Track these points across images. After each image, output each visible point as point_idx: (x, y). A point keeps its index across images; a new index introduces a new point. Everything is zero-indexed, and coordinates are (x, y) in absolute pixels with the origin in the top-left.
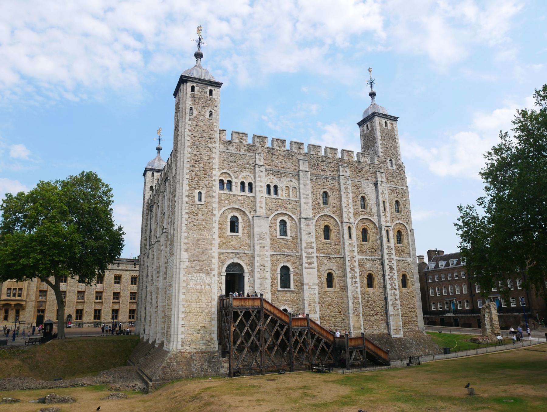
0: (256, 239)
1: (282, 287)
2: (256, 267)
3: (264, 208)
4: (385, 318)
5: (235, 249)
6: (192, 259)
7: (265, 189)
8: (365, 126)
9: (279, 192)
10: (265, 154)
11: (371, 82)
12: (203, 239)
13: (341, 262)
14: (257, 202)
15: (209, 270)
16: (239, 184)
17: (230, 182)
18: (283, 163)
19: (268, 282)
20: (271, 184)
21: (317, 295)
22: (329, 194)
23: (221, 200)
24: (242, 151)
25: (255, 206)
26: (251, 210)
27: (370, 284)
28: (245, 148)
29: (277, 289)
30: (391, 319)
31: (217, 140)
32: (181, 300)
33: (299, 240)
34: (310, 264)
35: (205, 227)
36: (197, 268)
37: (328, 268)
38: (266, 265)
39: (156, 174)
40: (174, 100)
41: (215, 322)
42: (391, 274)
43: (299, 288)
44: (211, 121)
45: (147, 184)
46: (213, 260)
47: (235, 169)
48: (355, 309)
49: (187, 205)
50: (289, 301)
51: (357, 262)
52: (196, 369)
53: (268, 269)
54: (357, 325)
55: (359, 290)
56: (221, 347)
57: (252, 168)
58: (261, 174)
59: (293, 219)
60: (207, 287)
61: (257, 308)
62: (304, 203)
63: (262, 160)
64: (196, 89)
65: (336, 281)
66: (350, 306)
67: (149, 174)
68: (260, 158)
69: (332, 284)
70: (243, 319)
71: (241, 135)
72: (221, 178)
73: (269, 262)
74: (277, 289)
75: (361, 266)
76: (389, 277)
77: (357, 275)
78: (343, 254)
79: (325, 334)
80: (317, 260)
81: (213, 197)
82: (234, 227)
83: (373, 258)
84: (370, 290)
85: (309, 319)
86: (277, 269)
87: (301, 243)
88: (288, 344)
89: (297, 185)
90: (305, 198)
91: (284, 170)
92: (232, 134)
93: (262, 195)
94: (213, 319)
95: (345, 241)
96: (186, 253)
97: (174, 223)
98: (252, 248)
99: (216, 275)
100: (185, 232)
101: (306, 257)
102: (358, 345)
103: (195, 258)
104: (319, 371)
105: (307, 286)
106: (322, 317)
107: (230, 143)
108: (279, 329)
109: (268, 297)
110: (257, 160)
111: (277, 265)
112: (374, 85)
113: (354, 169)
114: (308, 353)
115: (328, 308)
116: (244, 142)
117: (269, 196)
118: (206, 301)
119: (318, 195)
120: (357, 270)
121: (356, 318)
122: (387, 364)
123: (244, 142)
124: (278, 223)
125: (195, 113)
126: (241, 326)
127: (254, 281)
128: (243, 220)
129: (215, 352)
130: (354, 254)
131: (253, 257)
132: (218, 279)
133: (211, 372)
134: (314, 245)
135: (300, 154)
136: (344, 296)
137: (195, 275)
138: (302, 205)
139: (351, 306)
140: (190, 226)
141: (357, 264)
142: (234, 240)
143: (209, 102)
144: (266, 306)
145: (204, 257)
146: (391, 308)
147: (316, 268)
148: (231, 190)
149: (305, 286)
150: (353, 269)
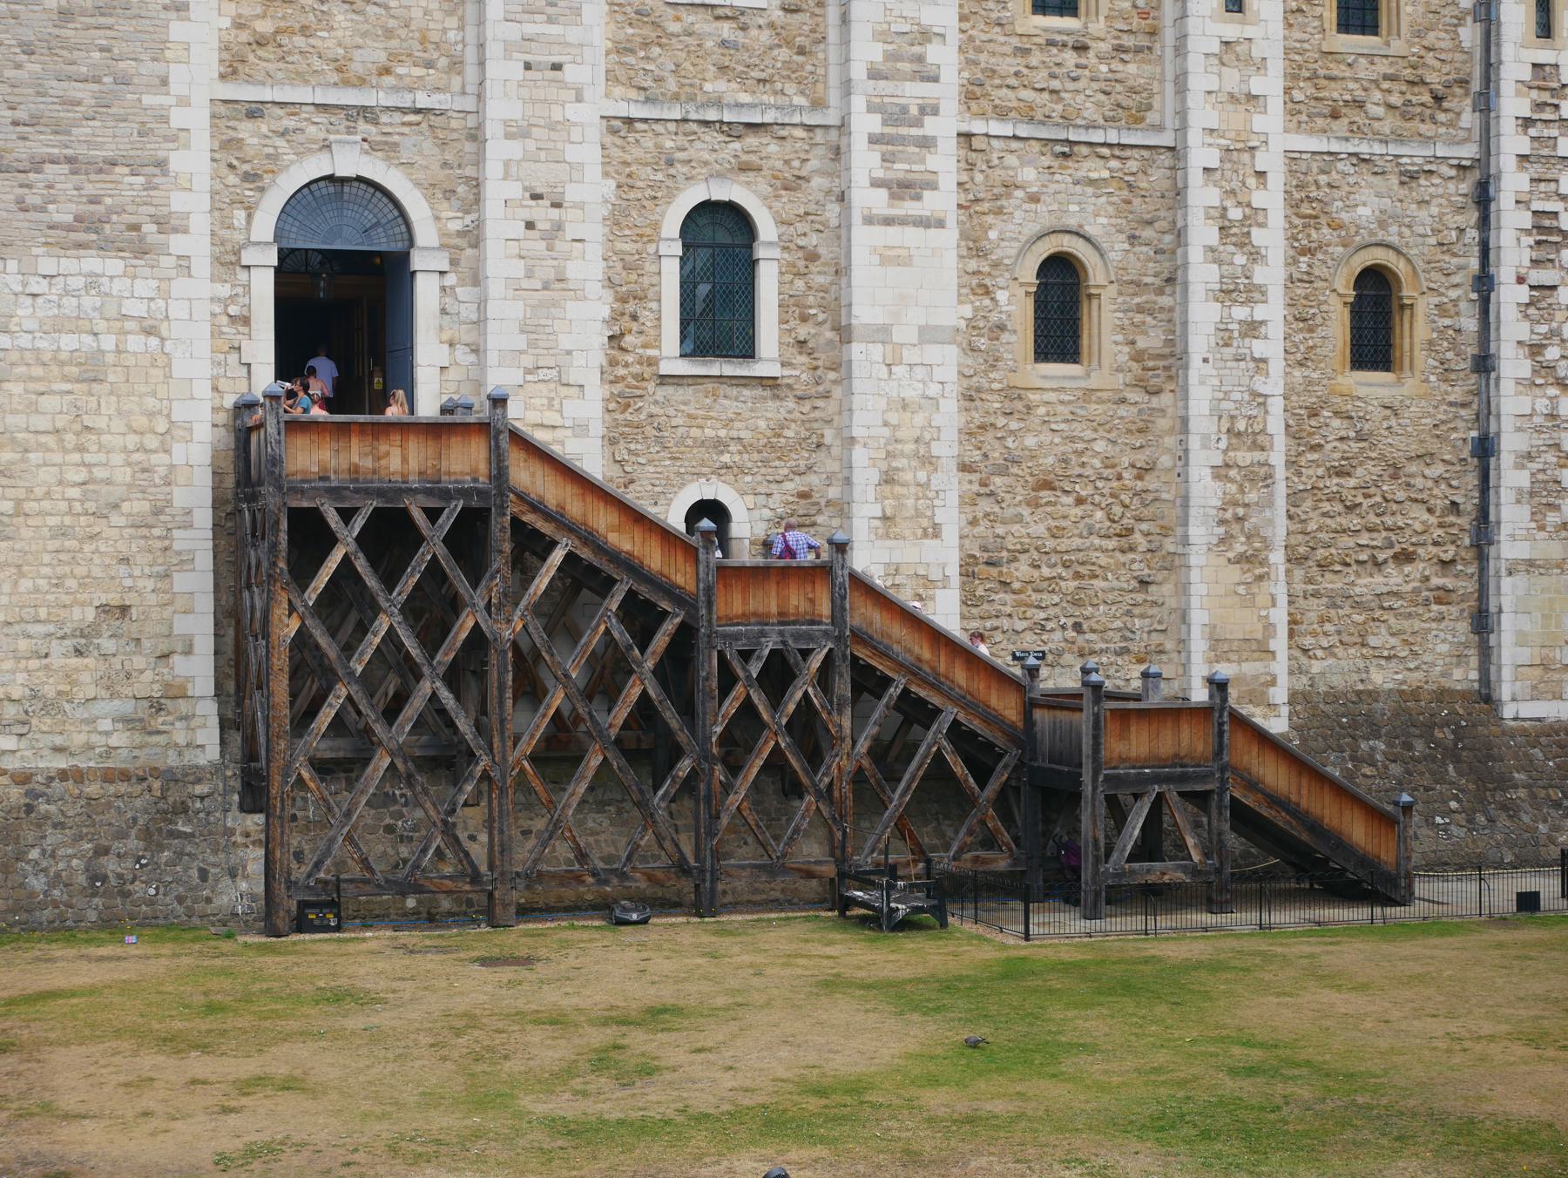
4: (1470, 586)
5: (346, 83)
13: (1157, 177)
15: (149, 228)
19: (585, 324)
27: (1373, 344)
29: (652, 362)
30: (1509, 592)
34: (904, 188)
37: (1047, 221)
38: (572, 194)
41: (197, 583)
42: (1537, 276)
43: (823, 359)
46: (178, 161)
48: (1233, 518)
50: (746, 448)
51: (1277, 180)
52: (56, 880)
54: (1242, 623)
55: (1273, 384)
56: (236, 738)
60: (135, 343)
61: (464, 493)
66: (1196, 491)
69: (1076, 336)
70: (361, 564)
73: (594, 171)
74: (652, 362)
75: (1307, 208)
76: (1523, 294)
77: (1272, 274)
78: (1171, 122)
79: (960, 676)
80: (971, 167)
83: (1414, 153)
84: (1372, 385)
85: (842, 576)
86: (656, 226)
87: (845, 42)
88: (683, 737)
94: (186, 562)
95: (1193, 24)
98: (471, 72)
99: (202, 265)
101: (874, 140)
102: (1177, 760)
103: (42, 144)
104: (879, 922)
105: (877, 351)
106: (982, 569)
108: (620, 634)
111: (659, 196)
114: (827, 795)
115: (1034, 504)
118: (132, 440)
120: (1272, 238)
121: (1235, 573)
122: (1372, 886)
126: (346, 603)
127: (482, 304)
129: (195, 775)
130: (1259, 123)
131: (476, 136)
132: (225, 290)
133: (151, 902)
134: (945, 57)
136: (1163, 423)
137: (47, 265)
139: (1205, 491)
141: (1272, 199)
144: (524, 475)
145: (105, 139)
146: (1511, 516)
147: (952, 218)
149: (857, 350)
150: (1236, 234)
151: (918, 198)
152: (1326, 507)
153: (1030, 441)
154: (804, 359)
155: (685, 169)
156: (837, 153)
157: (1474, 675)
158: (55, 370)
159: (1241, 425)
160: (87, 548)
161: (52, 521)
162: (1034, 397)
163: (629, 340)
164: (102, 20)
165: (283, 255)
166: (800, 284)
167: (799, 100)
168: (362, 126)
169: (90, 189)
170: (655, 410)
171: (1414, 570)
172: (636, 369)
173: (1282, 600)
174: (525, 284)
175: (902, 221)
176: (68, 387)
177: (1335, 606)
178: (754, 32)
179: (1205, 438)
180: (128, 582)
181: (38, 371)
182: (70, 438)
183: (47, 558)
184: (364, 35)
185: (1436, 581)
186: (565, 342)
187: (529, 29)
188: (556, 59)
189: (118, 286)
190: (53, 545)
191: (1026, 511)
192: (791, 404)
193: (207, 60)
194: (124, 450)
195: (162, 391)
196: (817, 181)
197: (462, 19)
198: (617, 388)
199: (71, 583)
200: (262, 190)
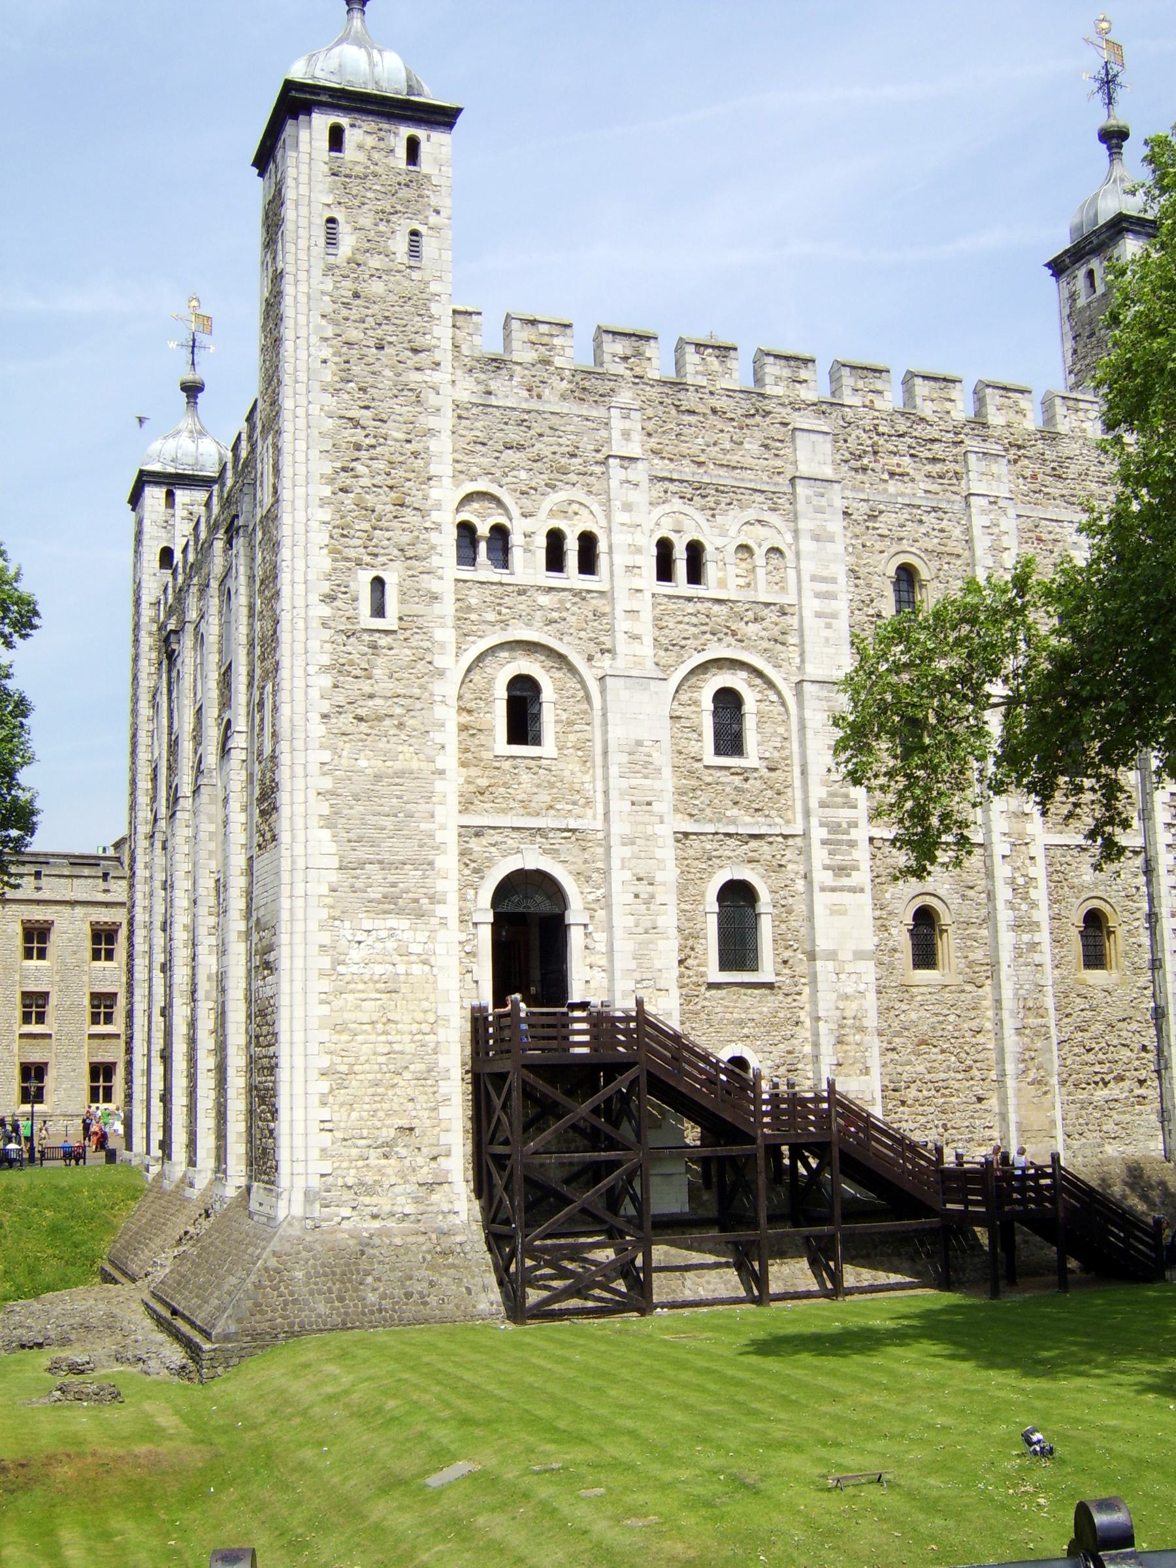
0: (614, 771)
1: (725, 965)
2: (616, 887)
3: (648, 640)
5: (529, 814)
6: (353, 856)
7: (649, 562)
8: (1081, 273)
9: (711, 571)
10: (650, 412)
11: (1108, 83)
12: (400, 774)
14: (619, 613)
16: (541, 541)
17: (500, 534)
18: (728, 445)
19: (668, 950)
20: (673, 537)
21: (871, 1001)
22: (925, 574)
23: (464, 610)
24: (551, 402)
25: (611, 631)
26: (593, 648)
28: (564, 385)
29: (703, 975)
31: (444, 354)
32: (314, 1023)
33: (797, 770)
34: (841, 870)
35: (401, 725)
36: (375, 893)
38: (659, 877)
39: (181, 496)
40: (255, 189)
44: (415, 275)
45: (146, 538)
46: (440, 862)
47: (523, 475)
48: (1027, 1058)
49: (327, 634)
51: (1041, 861)
53: (667, 896)
54: (1037, 1120)
57: (598, 469)
58: (634, 496)
59: (770, 684)
60: (417, 969)
62: (818, 615)
63: (637, 436)
64: (351, 137)
65: (948, 946)
67: (154, 495)
68: (627, 424)
71: (543, 328)
72: (464, 516)
73: (671, 864)
75: (1058, 877)
77: (1042, 915)
81: (435, 598)
82: (523, 719)
84: (1096, 976)
86: (703, 894)
89: (784, 541)
90: (818, 595)
91: (725, 478)
92: (506, 326)
93: (637, 583)
96: (326, 834)
97: (275, 709)
99: (454, 922)
100: (322, 747)
101: (824, 842)
103: (363, 853)
105: (830, 965)
106: (892, 1090)
107: (497, 364)
109: (667, 1009)
110: (616, 435)
111: (705, 875)
112: (1119, 95)
113: (1029, 467)
116: (558, 362)
117: (665, 588)
119: (876, 582)
120: (1040, 894)
123: (558, 362)
124: (708, 704)
125: (348, 242)
128: (559, 690)
135: (797, 406)
138: (810, 622)
139: (1011, 1042)
140: (345, 721)
141: (1039, 871)
142: (525, 777)
143: (404, 193)
145: (404, 850)
147: (868, 887)
148: (505, 564)
150: (1021, 891)
151: (849, 875)
152: (1076, 1050)
153: (913, 1016)
154: (786, 971)
155: (717, 861)
156: (805, 852)
157: (1161, 1146)
158: (371, 985)
159: (1030, 1004)
160: (390, 1093)
161: (370, 1077)
162: (915, 990)
163: (690, 962)
164: (397, 780)
165: (496, 915)
166: (783, 926)
167: (778, 820)
168: (538, 839)
169: (392, 879)
170: (706, 1003)
171: (1126, 1084)
172: (694, 979)
173: (1058, 1105)
174: (635, 930)
175: (841, 889)
176: (378, 996)
177: (1082, 1108)
178: (751, 781)
179: (1012, 1011)
180: (414, 1113)
181: (361, 986)
182: (380, 1026)
183: (367, 1099)
184: (538, 786)
185: (1138, 1092)
186: (658, 965)
187: (634, 782)
188: (648, 799)
189: (406, 936)
190: (371, 1091)
191: (913, 1058)
192: (781, 997)
193: (453, 801)
194: (411, 1033)
195: (432, 997)
196: (790, 867)
197: (594, 776)
198: (684, 991)
199: (381, 1114)
200: (482, 878)
